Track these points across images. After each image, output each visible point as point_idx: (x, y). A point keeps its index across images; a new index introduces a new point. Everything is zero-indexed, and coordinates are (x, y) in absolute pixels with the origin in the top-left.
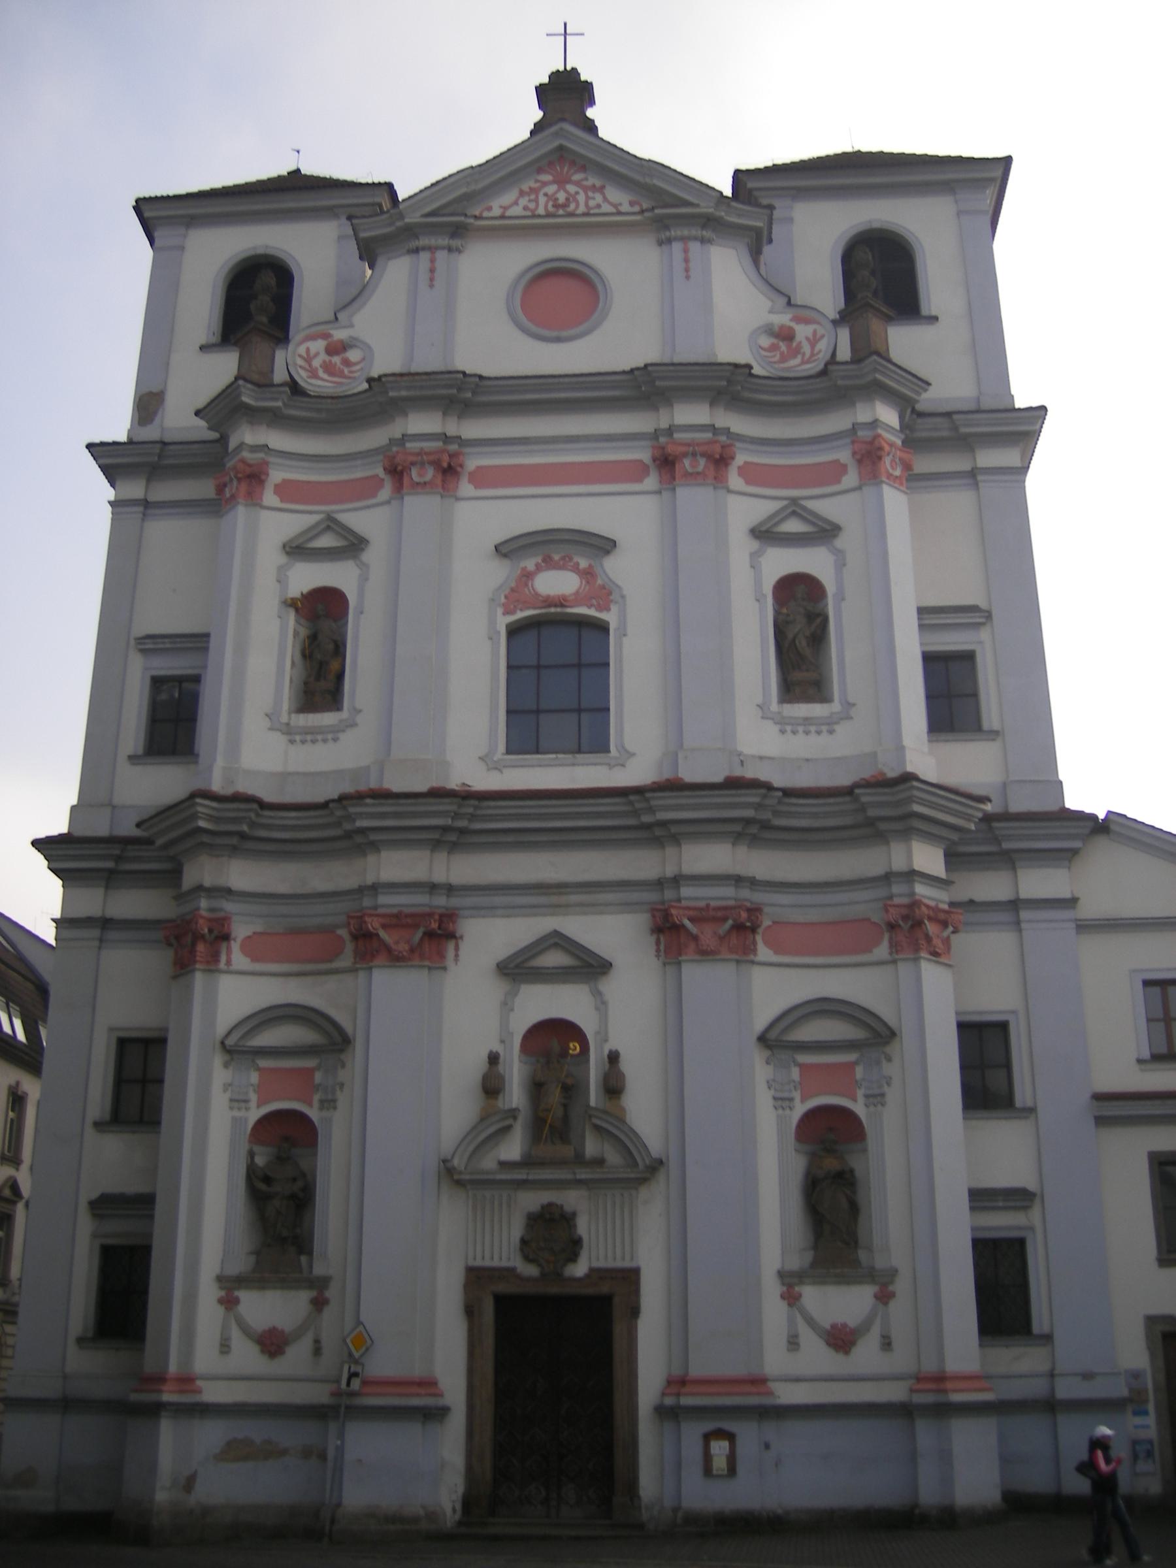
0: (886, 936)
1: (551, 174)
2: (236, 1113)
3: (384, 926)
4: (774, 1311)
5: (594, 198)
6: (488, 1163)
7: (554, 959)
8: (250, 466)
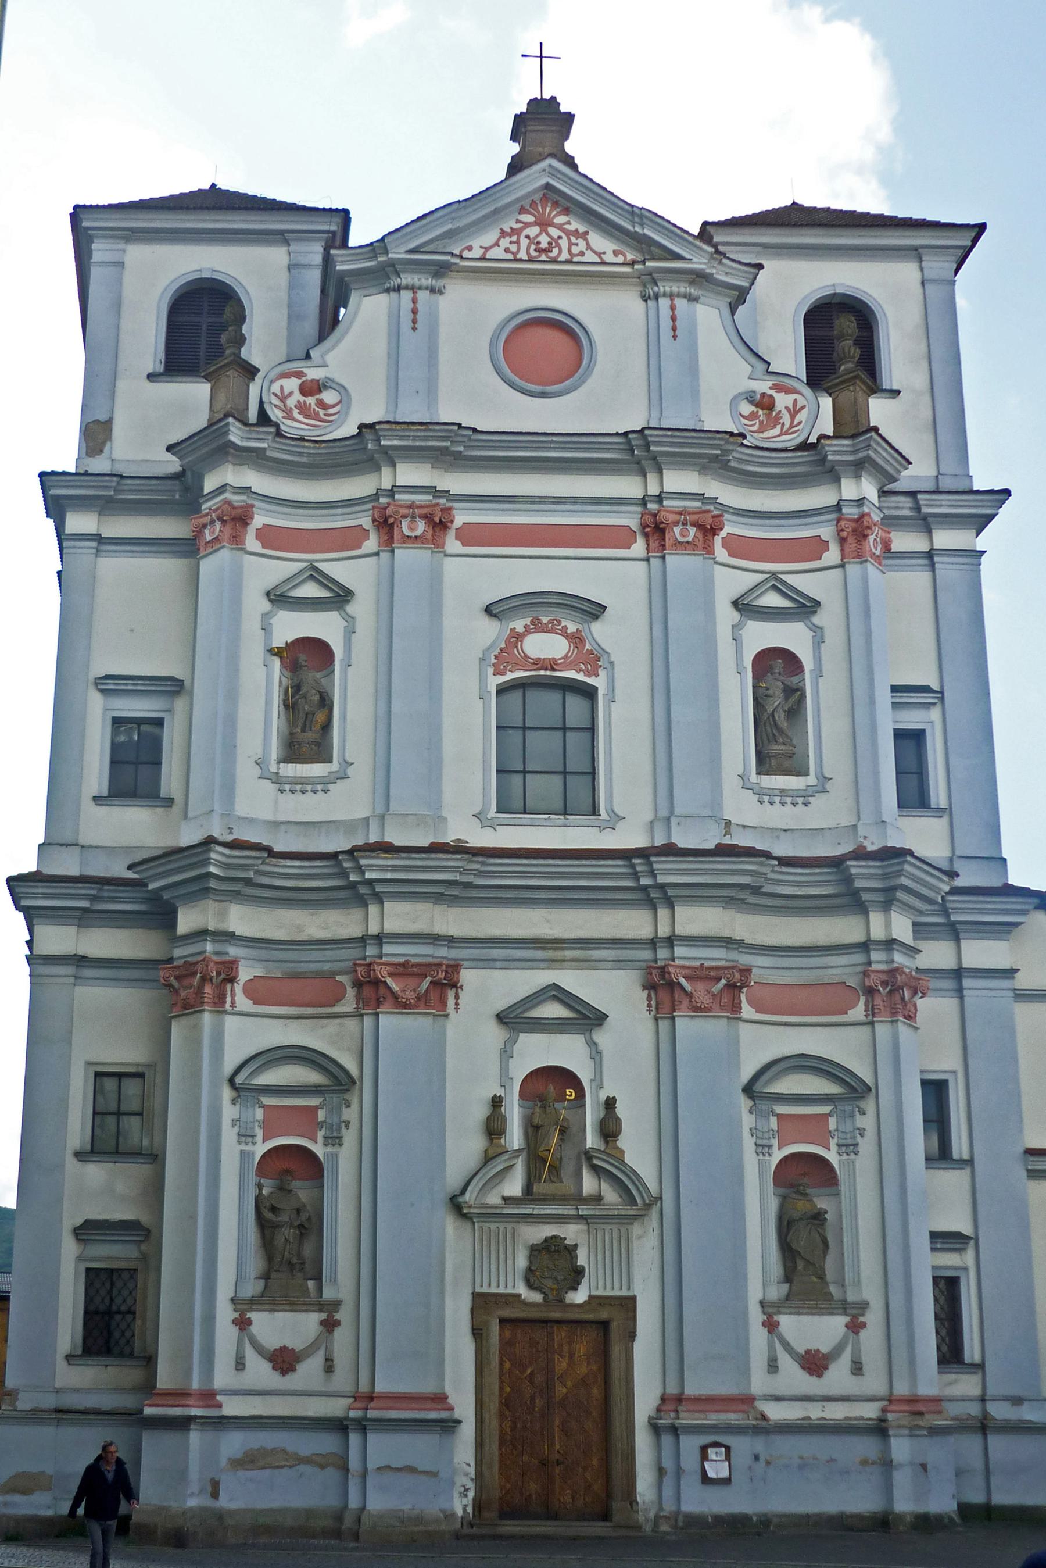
0: (862, 999)
1: (533, 215)
2: (243, 1147)
3: (390, 975)
4: (758, 1336)
5: (577, 244)
6: (493, 1199)
7: (553, 1010)
8: (234, 508)
